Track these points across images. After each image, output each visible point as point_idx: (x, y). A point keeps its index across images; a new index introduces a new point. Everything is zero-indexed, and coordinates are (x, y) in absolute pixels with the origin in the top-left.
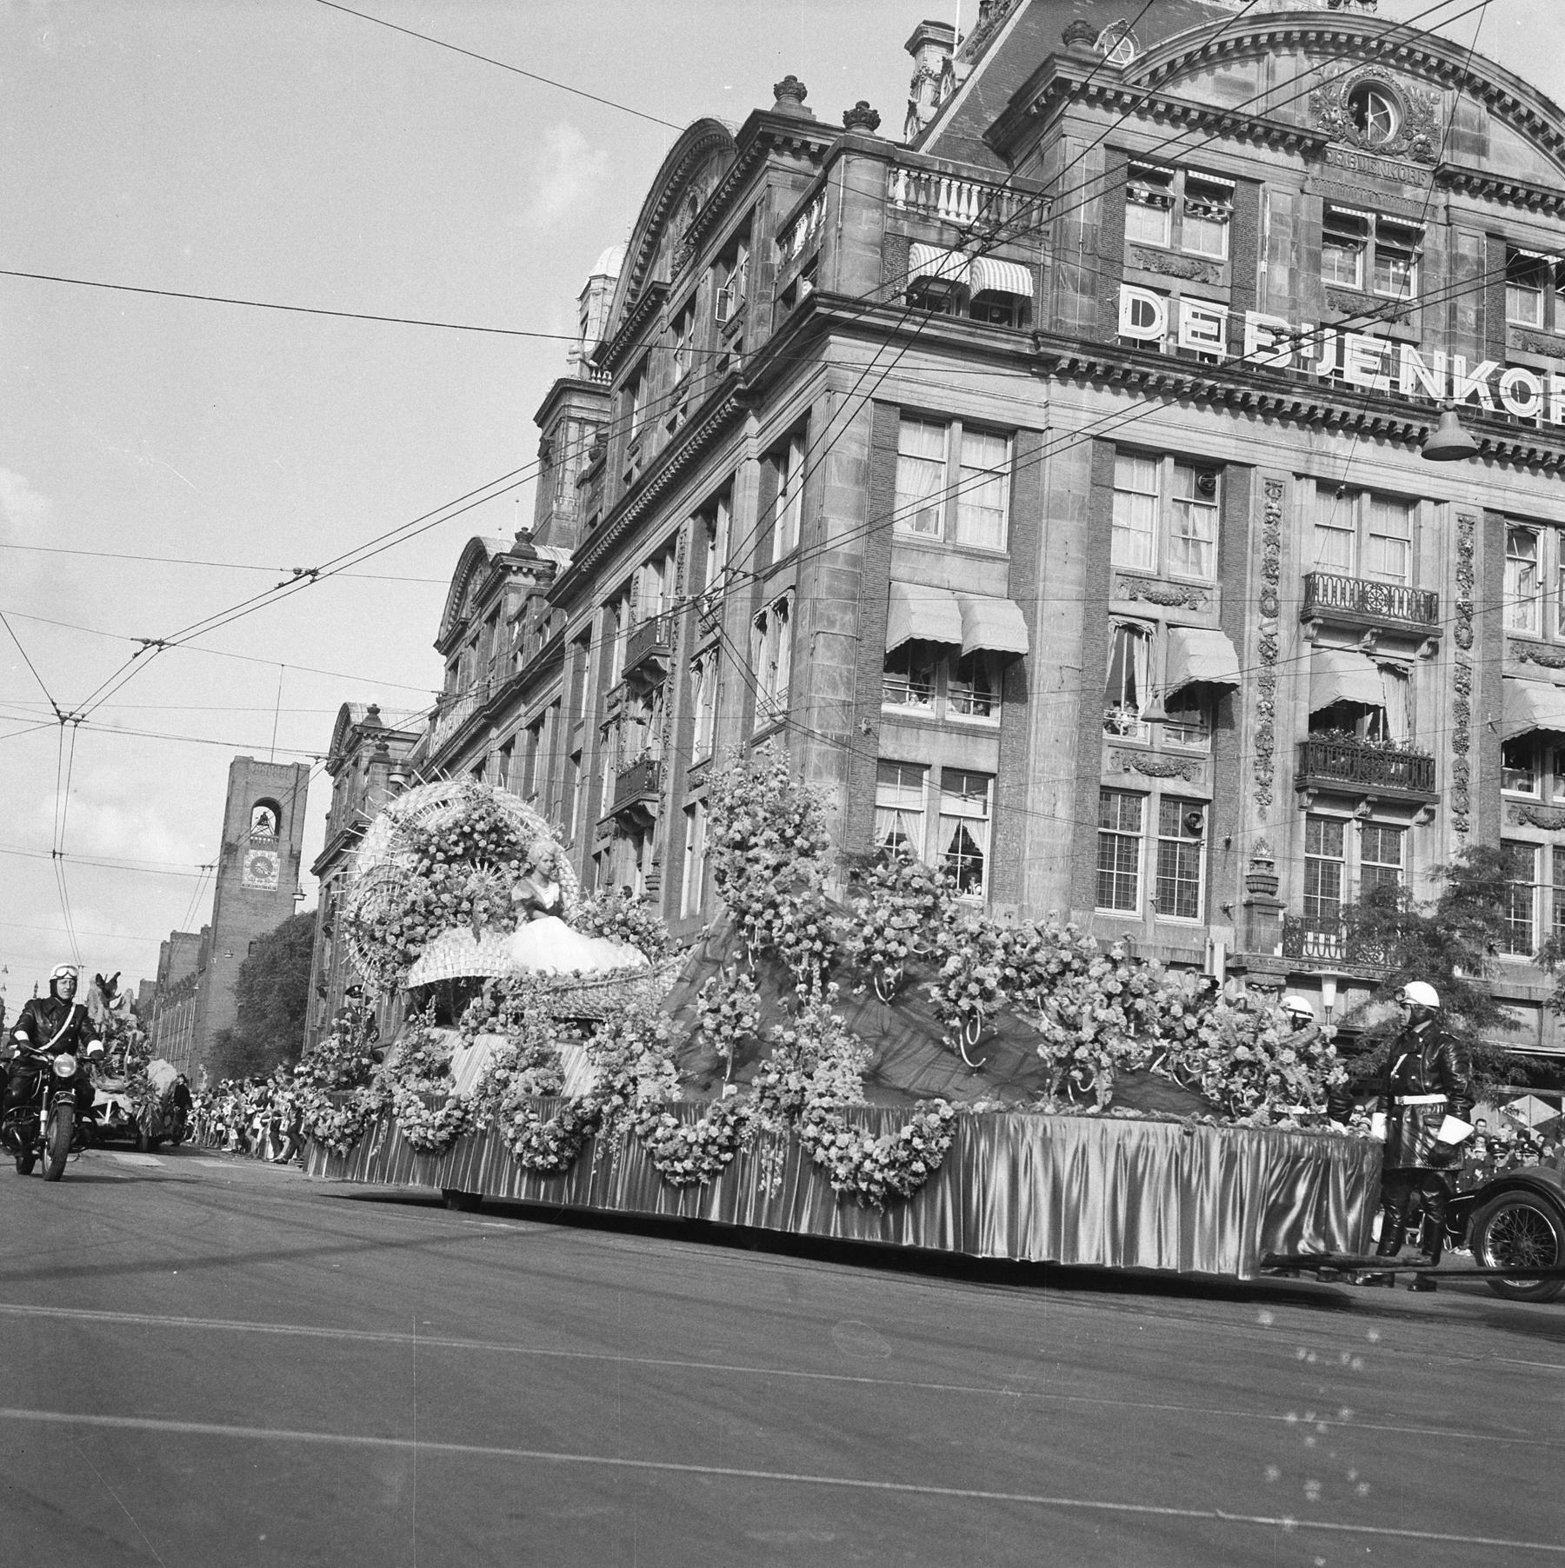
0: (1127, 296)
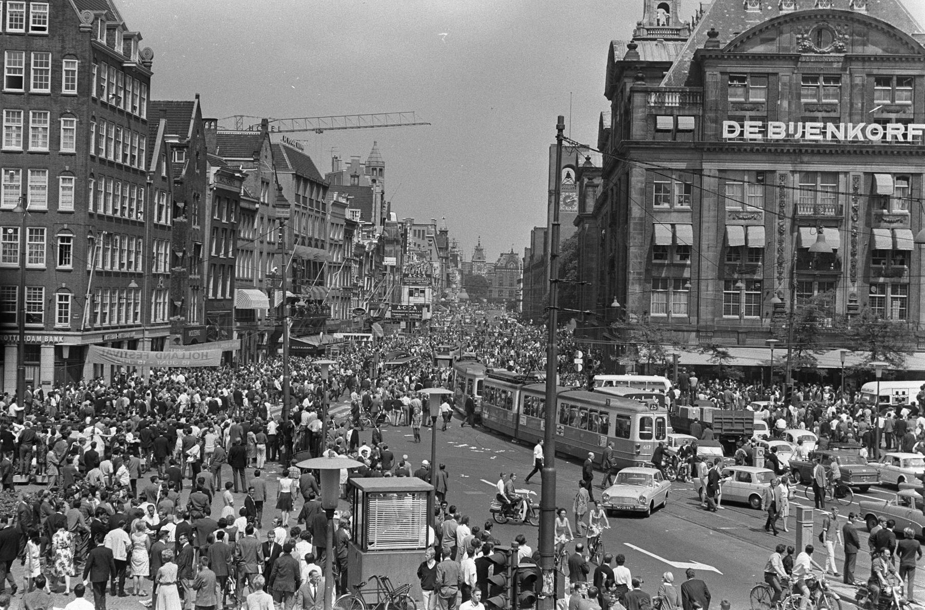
0: (726, 124)
